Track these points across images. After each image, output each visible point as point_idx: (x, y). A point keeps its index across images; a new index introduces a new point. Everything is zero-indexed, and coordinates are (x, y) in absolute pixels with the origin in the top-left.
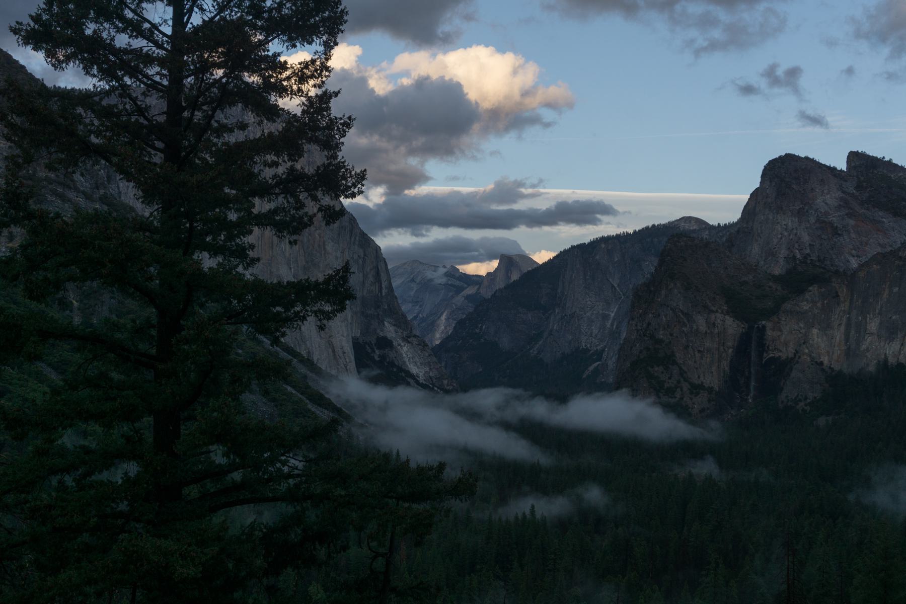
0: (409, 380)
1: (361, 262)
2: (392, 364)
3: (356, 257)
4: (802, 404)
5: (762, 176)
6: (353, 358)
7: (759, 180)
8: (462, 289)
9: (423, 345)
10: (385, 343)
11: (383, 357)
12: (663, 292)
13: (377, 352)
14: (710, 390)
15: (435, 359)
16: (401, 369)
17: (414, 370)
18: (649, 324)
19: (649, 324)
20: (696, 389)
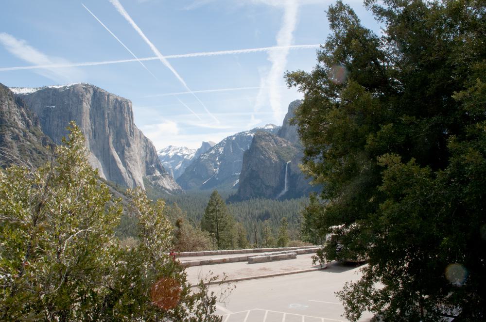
0: (166, 191)
1: (145, 148)
2: (159, 186)
3: (143, 146)
4: (305, 190)
5: (289, 108)
6: (143, 184)
7: (288, 109)
8: (189, 155)
9: (171, 178)
10: (156, 178)
11: (156, 183)
12: (254, 153)
13: (154, 182)
14: (272, 187)
15: (175, 183)
16: (162, 187)
17: (168, 187)
18: (250, 164)
19: (250, 164)
20: (267, 187)
